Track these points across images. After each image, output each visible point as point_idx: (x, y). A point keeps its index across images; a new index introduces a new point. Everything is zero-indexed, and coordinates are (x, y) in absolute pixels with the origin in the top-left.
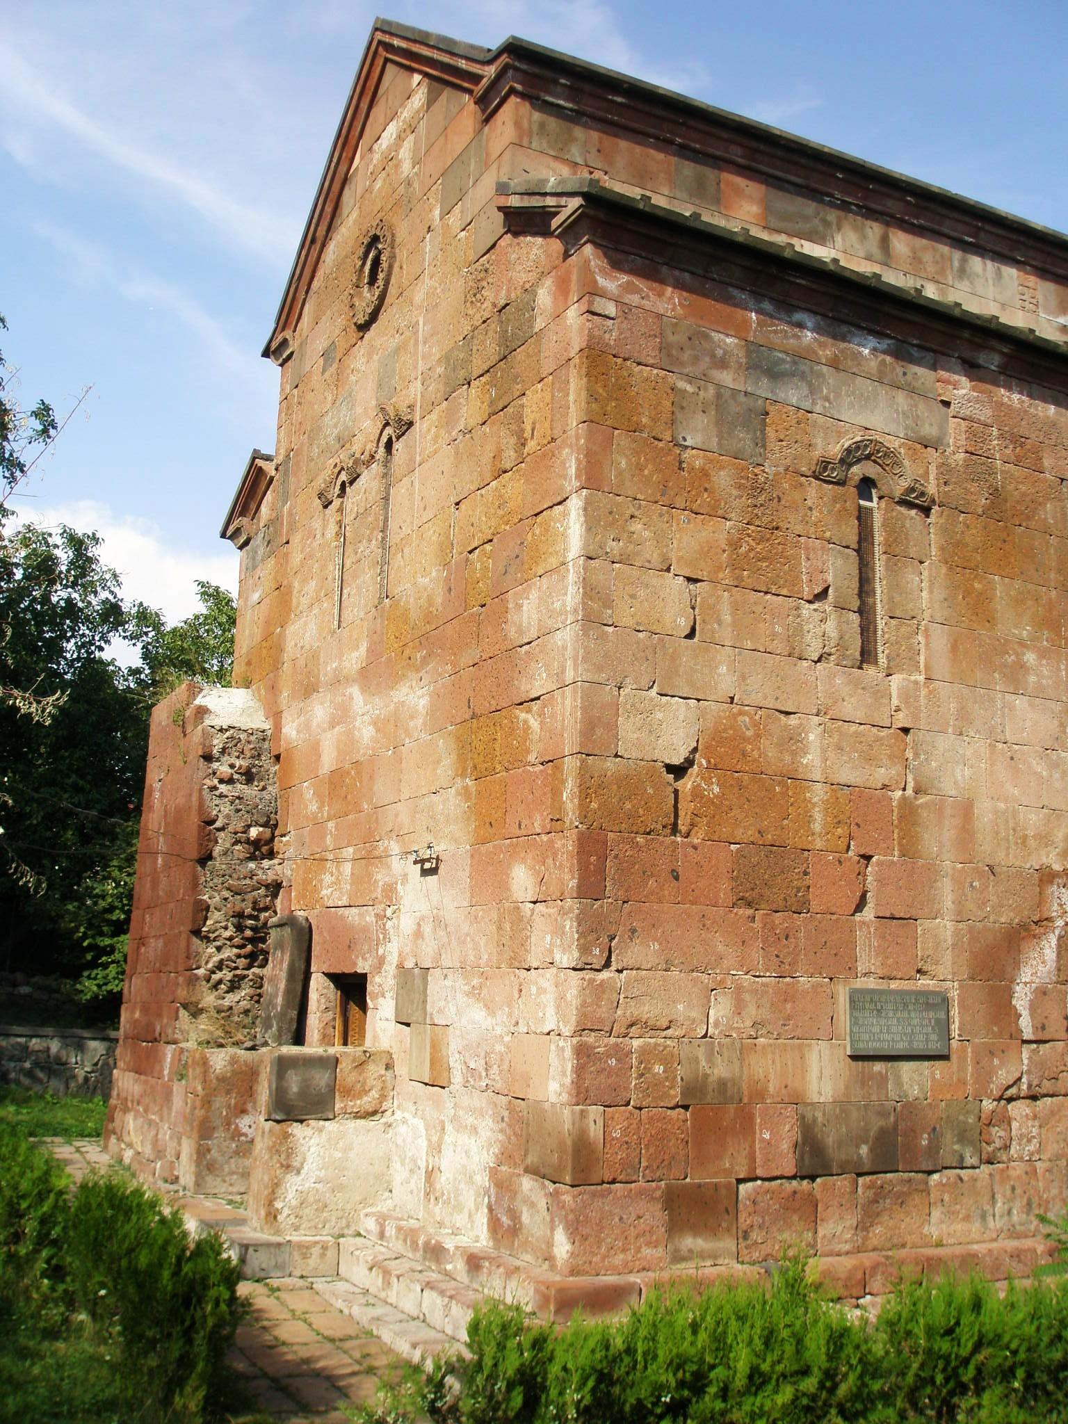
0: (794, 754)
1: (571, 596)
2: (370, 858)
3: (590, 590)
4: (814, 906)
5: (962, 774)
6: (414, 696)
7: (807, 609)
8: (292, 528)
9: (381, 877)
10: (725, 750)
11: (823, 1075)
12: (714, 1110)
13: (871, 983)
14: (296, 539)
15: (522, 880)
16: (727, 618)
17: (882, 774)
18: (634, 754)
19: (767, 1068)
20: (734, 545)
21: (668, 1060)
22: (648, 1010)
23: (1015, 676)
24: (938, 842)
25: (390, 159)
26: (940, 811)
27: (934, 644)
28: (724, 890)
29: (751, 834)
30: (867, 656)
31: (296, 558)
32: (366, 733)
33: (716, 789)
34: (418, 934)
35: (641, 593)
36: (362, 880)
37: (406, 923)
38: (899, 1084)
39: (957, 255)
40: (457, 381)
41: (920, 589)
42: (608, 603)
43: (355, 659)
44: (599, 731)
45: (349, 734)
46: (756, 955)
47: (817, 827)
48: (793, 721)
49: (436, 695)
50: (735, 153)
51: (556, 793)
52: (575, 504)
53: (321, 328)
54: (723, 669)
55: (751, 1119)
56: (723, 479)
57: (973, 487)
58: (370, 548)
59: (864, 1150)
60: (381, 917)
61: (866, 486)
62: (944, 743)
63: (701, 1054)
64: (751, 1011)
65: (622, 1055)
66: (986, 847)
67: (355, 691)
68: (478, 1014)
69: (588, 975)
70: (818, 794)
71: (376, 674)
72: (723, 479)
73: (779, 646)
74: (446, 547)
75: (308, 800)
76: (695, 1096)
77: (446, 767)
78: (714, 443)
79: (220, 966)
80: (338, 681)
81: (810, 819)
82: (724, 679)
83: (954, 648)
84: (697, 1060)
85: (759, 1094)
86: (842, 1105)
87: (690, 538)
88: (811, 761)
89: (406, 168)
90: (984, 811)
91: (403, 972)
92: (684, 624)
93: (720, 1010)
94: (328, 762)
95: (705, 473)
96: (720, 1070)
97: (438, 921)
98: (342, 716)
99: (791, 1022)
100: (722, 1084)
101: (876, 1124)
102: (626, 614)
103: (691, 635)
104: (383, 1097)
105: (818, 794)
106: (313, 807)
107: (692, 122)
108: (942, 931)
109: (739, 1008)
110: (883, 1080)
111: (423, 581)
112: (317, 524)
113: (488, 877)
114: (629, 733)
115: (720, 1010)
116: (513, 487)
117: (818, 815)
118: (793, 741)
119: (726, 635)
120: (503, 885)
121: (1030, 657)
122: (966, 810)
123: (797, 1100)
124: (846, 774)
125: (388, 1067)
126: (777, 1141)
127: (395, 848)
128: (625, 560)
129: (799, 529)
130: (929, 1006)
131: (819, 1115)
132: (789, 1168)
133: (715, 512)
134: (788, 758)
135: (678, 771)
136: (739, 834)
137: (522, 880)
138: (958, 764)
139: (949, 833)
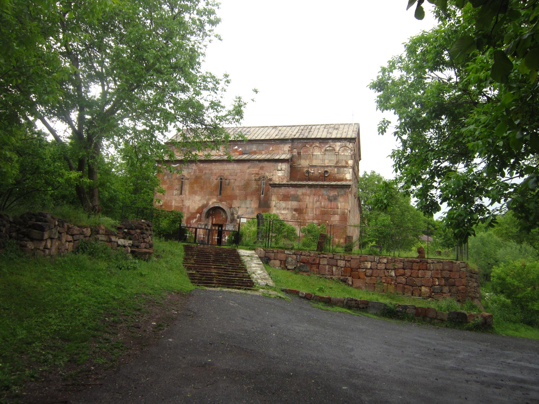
5: (188, 204)
24: (185, 210)
27: (187, 192)
30: (181, 194)
41: (186, 187)
56: (168, 181)
61: (182, 179)
62: (187, 201)
72: (168, 181)
83: (189, 192)
88: (173, 204)
90: (191, 207)
118: (172, 203)
122: (189, 207)
138: (187, 203)
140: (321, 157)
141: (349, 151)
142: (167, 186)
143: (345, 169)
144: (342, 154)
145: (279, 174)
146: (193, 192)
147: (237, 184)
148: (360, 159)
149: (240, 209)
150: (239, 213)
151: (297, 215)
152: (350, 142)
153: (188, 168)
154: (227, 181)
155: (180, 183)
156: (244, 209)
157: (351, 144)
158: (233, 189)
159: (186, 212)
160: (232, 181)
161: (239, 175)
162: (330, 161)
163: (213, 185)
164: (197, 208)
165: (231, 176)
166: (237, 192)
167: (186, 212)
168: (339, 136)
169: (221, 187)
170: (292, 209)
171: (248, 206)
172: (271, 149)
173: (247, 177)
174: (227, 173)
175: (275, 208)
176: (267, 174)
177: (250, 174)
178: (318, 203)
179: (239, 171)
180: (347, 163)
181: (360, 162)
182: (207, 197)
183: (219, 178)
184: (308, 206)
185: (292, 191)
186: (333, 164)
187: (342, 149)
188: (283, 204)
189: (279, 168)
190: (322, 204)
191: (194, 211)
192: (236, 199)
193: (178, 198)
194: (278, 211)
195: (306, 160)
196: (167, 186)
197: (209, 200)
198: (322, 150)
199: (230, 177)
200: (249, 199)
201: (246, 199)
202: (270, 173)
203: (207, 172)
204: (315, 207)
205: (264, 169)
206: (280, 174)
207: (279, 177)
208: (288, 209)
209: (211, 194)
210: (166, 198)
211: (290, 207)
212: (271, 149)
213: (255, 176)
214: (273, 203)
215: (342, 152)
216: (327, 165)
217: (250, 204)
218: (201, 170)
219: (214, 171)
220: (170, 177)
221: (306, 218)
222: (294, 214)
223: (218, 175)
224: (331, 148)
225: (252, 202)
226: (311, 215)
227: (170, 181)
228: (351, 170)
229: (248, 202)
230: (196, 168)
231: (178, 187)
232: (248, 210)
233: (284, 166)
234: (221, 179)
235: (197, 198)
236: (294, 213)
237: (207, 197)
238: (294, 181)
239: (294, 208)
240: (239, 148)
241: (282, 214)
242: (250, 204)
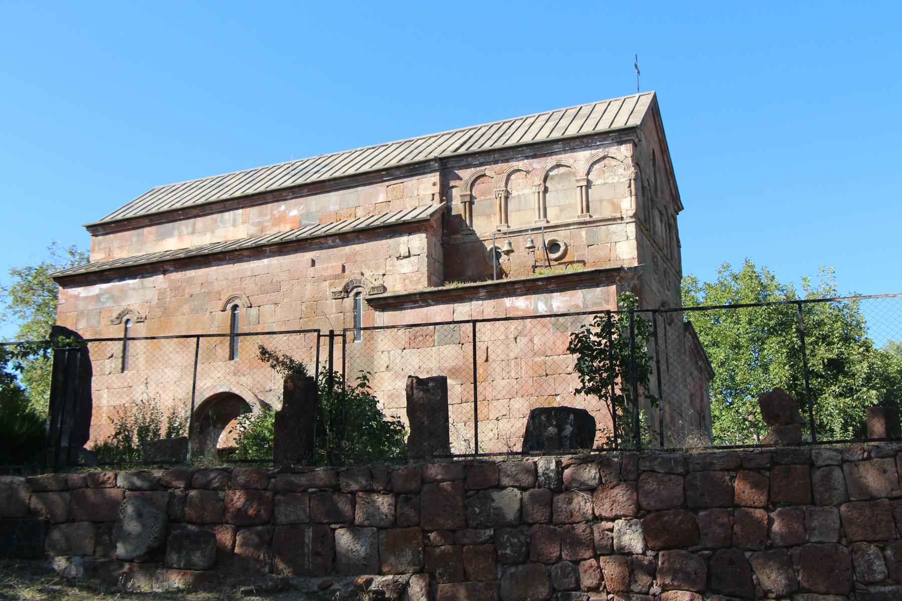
17: (124, 401)
39: (220, 215)
50: (147, 222)
105: (105, 408)
140: (534, 200)
141: (621, 171)
143: (613, 228)
144: (600, 182)
145: (406, 265)
148: (680, 208)
152: (621, 143)
153: (143, 288)
154: (254, 311)
157: (623, 147)
162: (562, 209)
168: (588, 129)
173: (309, 291)
174: (250, 287)
175: (388, 375)
178: (522, 341)
180: (616, 207)
181: (682, 219)
183: (229, 306)
184: (492, 357)
185: (438, 312)
186: (575, 214)
187: (596, 167)
189: (403, 251)
190: (536, 340)
195: (488, 216)
198: (538, 180)
202: (377, 269)
203: (197, 290)
204: (512, 355)
205: (358, 258)
206: (406, 267)
207: (405, 277)
212: (381, 198)
213: (331, 285)
215: (599, 176)
216: (552, 224)
219: (216, 286)
220: (94, 321)
223: (225, 298)
226: (500, 383)
228: (631, 229)
230: (166, 286)
233: (418, 242)
238: (451, 281)
240: (289, 209)
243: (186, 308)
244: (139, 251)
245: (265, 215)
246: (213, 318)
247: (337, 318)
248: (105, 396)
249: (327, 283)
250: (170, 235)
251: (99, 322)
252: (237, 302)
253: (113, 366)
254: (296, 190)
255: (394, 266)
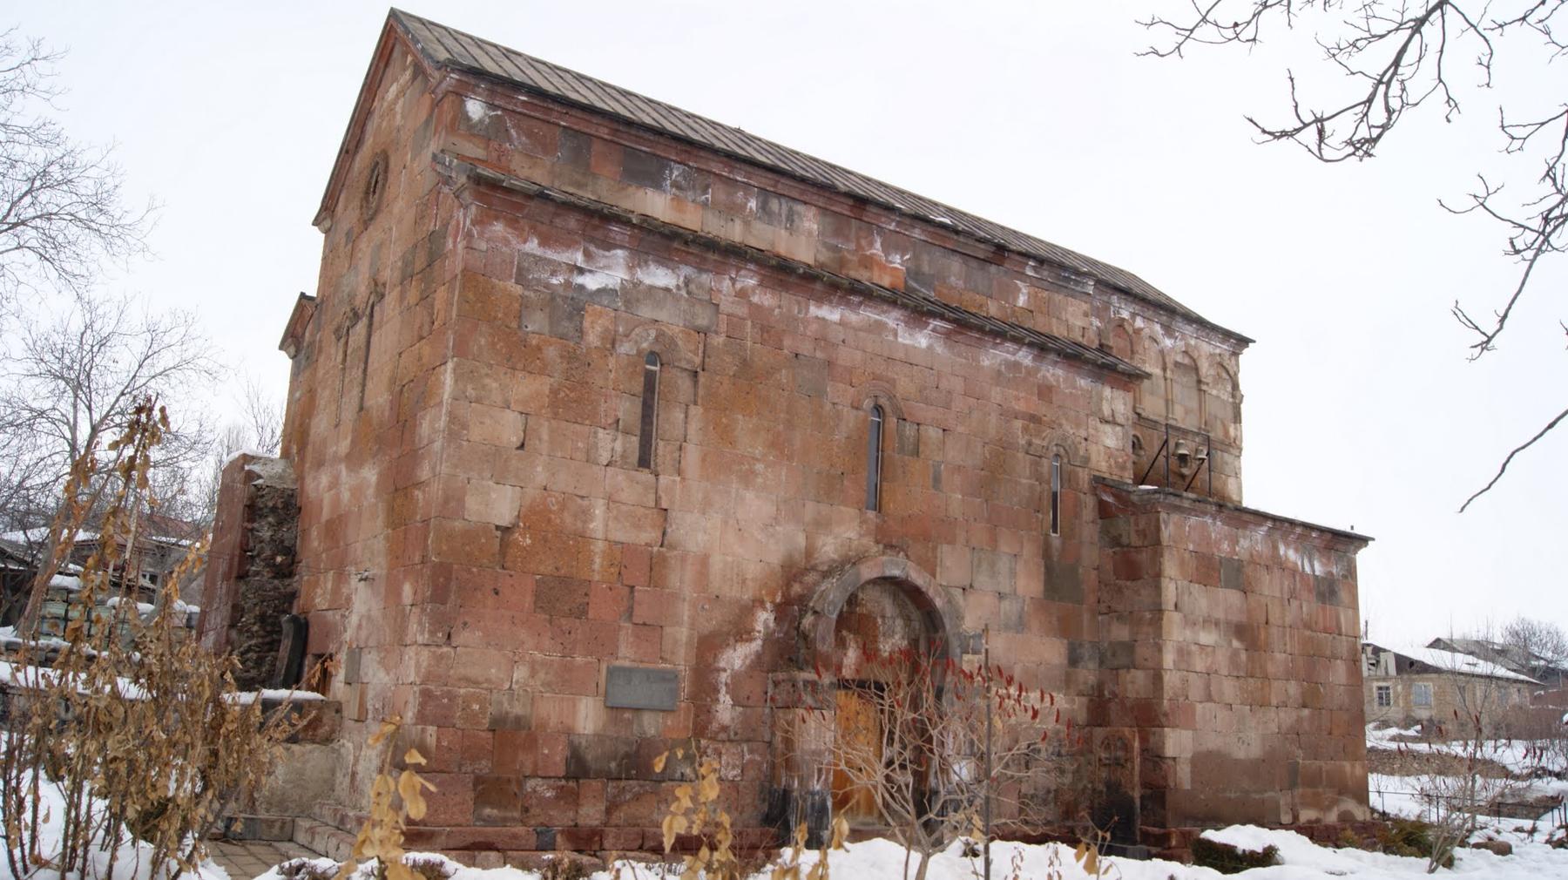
0: (585, 522)
1: (442, 423)
2: (341, 577)
3: (453, 417)
4: (590, 615)
6: (370, 474)
7: (601, 433)
8: (320, 351)
9: (345, 590)
10: (534, 517)
11: (588, 718)
12: (510, 733)
13: (627, 664)
14: (321, 359)
15: (407, 590)
16: (545, 437)
18: (474, 519)
19: (550, 710)
20: (554, 392)
21: (483, 703)
22: (473, 672)
23: (747, 478)
24: (681, 580)
25: (391, 109)
26: (683, 559)
28: (528, 601)
29: (547, 568)
31: (321, 373)
32: (346, 496)
33: (529, 541)
34: (360, 626)
35: (488, 421)
36: (336, 591)
37: (354, 619)
38: (641, 726)
40: (406, 277)
41: (683, 422)
42: (465, 426)
43: (344, 446)
44: (453, 504)
45: (338, 495)
46: (547, 643)
47: (596, 567)
48: (586, 502)
49: (380, 475)
51: (426, 539)
52: (450, 365)
53: (349, 214)
54: (539, 469)
55: (535, 740)
56: (551, 353)
57: (728, 359)
58: (357, 373)
59: (613, 765)
60: (343, 616)
61: (653, 357)
63: (505, 699)
64: (542, 675)
65: (452, 697)
66: (716, 584)
67: (343, 467)
68: (382, 674)
69: (433, 649)
70: (599, 546)
71: (354, 460)
72: (551, 353)
73: (580, 455)
74: (393, 380)
75: (315, 540)
76: (499, 725)
77: (380, 521)
78: (546, 330)
79: (249, 650)
80: (336, 459)
81: (592, 562)
82: (540, 475)
83: (704, 460)
84: (501, 703)
85: (543, 726)
86: (599, 737)
87: (526, 387)
88: (597, 526)
89: (398, 120)
91: (351, 652)
92: (516, 440)
93: (520, 673)
94: (326, 514)
95: (539, 349)
96: (517, 710)
97: (369, 618)
98: (335, 484)
99: (567, 682)
100: (518, 719)
101: (623, 749)
102: (476, 434)
103: (522, 446)
104: (333, 731)
105: (599, 546)
106: (316, 544)
107: (573, 112)
108: (681, 635)
109: (533, 673)
110: (630, 722)
111: (381, 400)
112: (333, 351)
113: (393, 592)
114: (473, 505)
115: (520, 673)
116: (425, 349)
117: (598, 560)
118: (586, 514)
119: (544, 448)
120: (399, 595)
121: (759, 467)
122: (704, 561)
123: (569, 732)
124: (619, 535)
125: (338, 711)
126: (557, 756)
127: (353, 569)
128: (478, 400)
129: (601, 383)
130: (664, 680)
131: (584, 743)
132: (562, 773)
133: (542, 371)
134: (579, 524)
135: (506, 530)
136: (542, 569)
137: (407, 590)
138: (697, 531)
139: (690, 573)
142: (543, 385)
146: (725, 463)
147: (954, 453)
149: (971, 598)
150: (970, 624)
151: (1243, 656)
154: (909, 430)
155: (638, 385)
156: (989, 600)
158: (937, 480)
159: (688, 592)
160: (933, 433)
161: (959, 404)
163: (840, 436)
164: (753, 570)
165: (927, 401)
166: (955, 500)
167: (688, 592)
169: (879, 452)
170: (1228, 623)
171: (1005, 588)
172: (1022, 301)
174: (905, 385)
175: (1177, 616)
176: (1069, 429)
177: (1008, 414)
179: (958, 385)
182: (810, 510)
183: (868, 404)
184: (1271, 620)
188: (1201, 600)
191: (732, 592)
192: (952, 542)
193: (630, 486)
194: (1188, 634)
196: (543, 385)
197: (821, 524)
199: (922, 411)
200: (1004, 548)
201: (994, 541)
202: (1078, 426)
203: (806, 348)
208: (1217, 624)
209: (830, 487)
210: (540, 475)
211: (1219, 614)
212: (1022, 301)
213: (1025, 429)
214: (1170, 591)
217: (1013, 574)
218: (768, 330)
221: (1271, 669)
222: (1235, 653)
224: (1186, 361)
225: (1020, 567)
226: (1279, 656)
227: (570, 357)
229: (1003, 565)
231: (627, 409)
232: (1006, 605)
234: (878, 409)
235: (755, 505)
236: (1236, 644)
237: (810, 510)
239: (1236, 617)
241: (1202, 647)
242: (1013, 574)
243: (784, 376)
244: (580, 186)
245: (847, 239)
246: (838, 416)
247: (1031, 487)
248: (599, 511)
249: (1018, 424)
250: (656, 183)
251: (581, 332)
252: (883, 401)
253: (618, 446)
254: (908, 221)
255: (1096, 429)
